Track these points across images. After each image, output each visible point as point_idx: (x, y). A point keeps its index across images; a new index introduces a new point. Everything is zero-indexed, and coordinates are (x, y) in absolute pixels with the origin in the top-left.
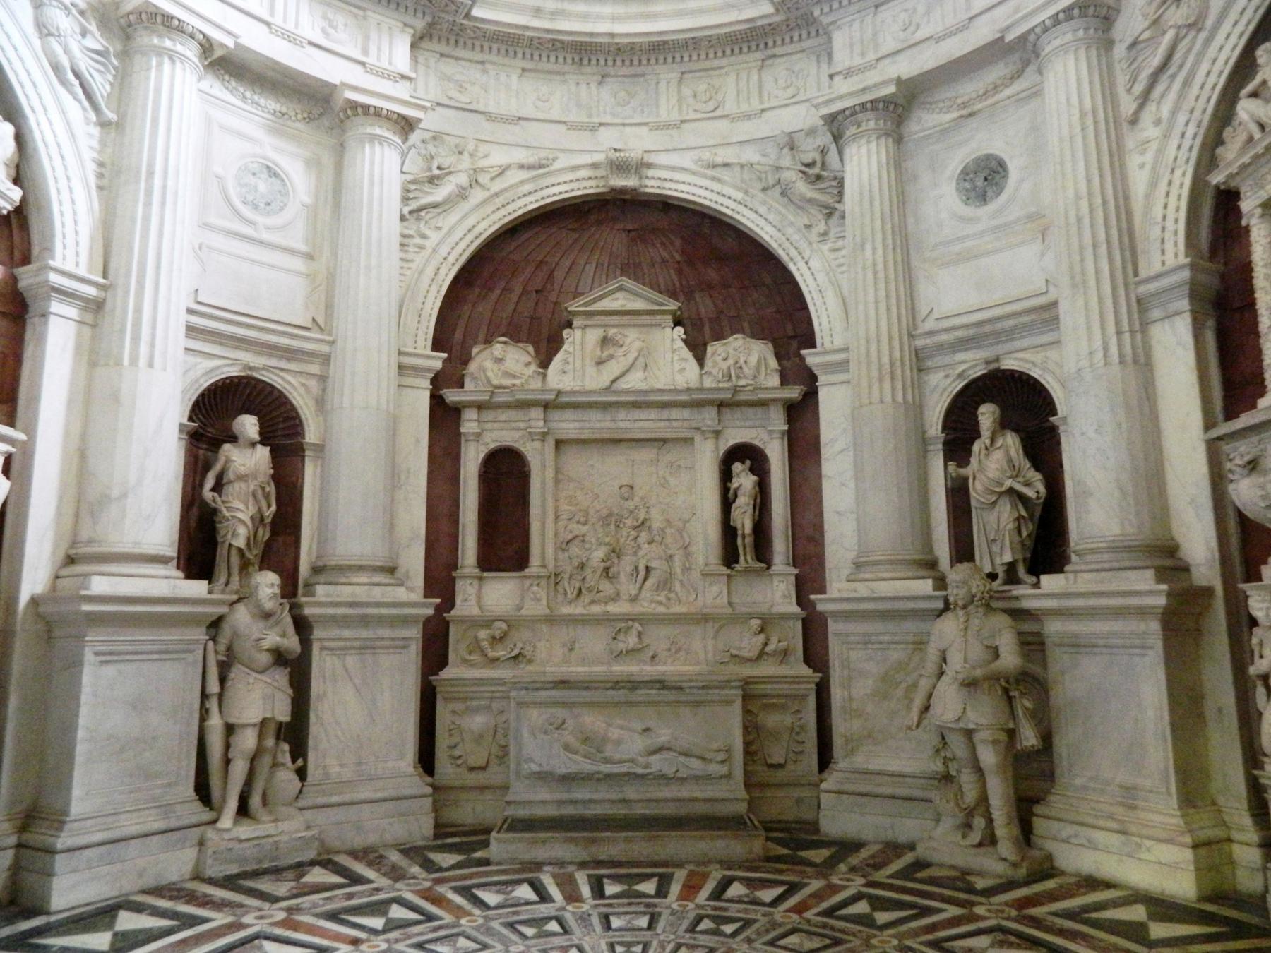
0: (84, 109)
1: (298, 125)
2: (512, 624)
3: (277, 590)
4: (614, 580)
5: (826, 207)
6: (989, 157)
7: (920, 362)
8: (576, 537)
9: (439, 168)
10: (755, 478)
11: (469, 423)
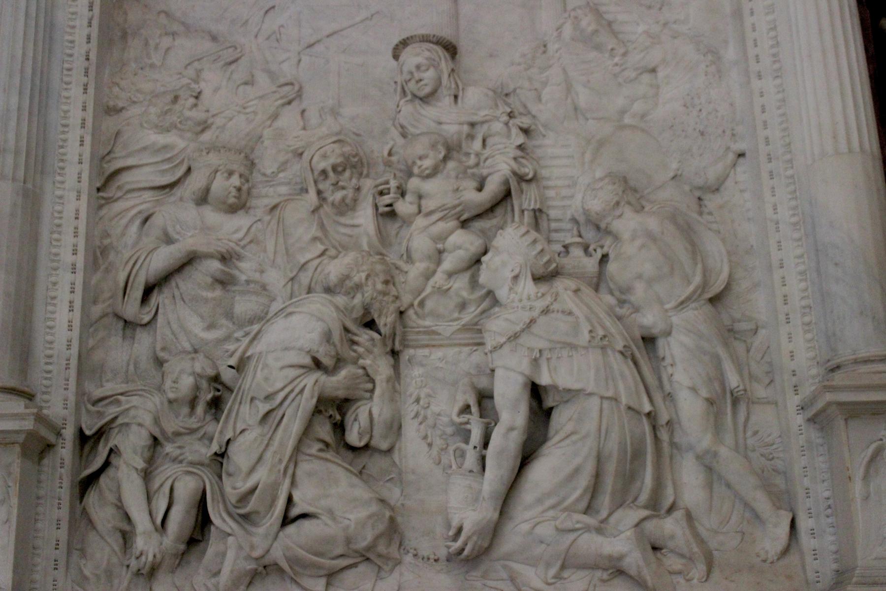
4: (375, 464)
8: (189, 261)
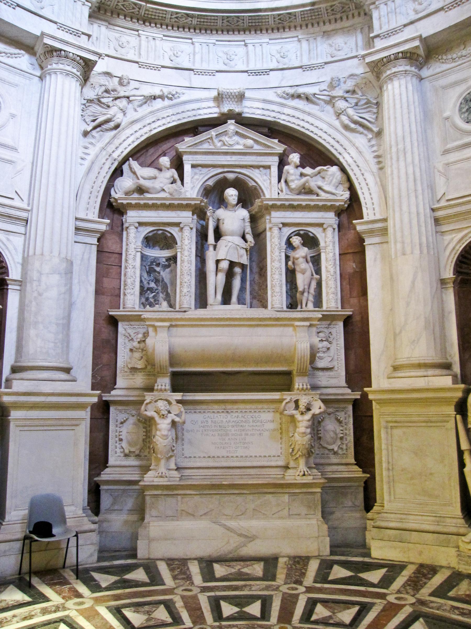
0: (366, 135)
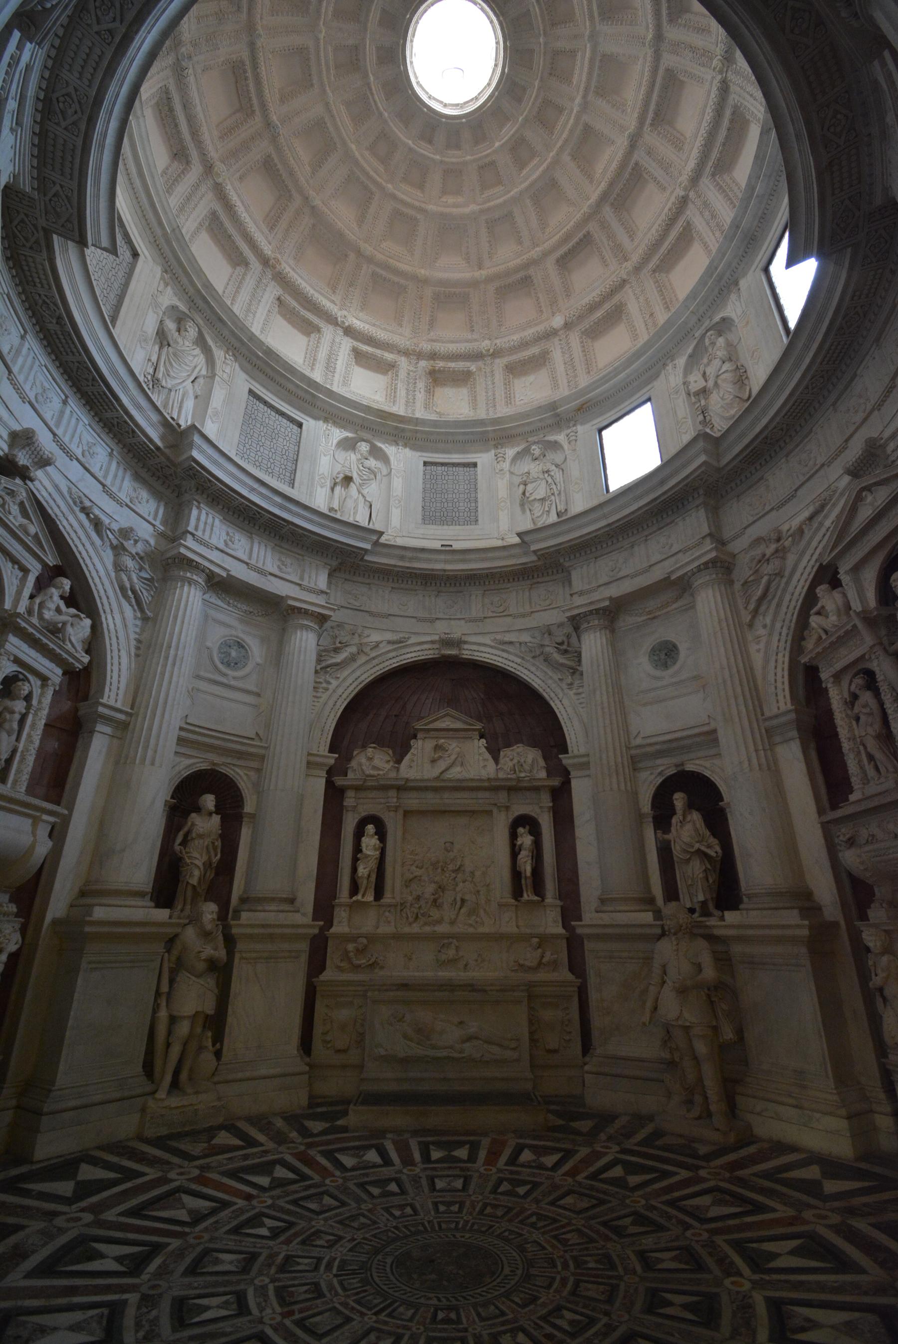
0: (135, 611)
1: (259, 619)
2: (372, 939)
3: (215, 916)
5: (572, 668)
6: (667, 642)
7: (635, 763)
8: (416, 877)
9: (340, 643)
10: (532, 838)
11: (350, 800)
